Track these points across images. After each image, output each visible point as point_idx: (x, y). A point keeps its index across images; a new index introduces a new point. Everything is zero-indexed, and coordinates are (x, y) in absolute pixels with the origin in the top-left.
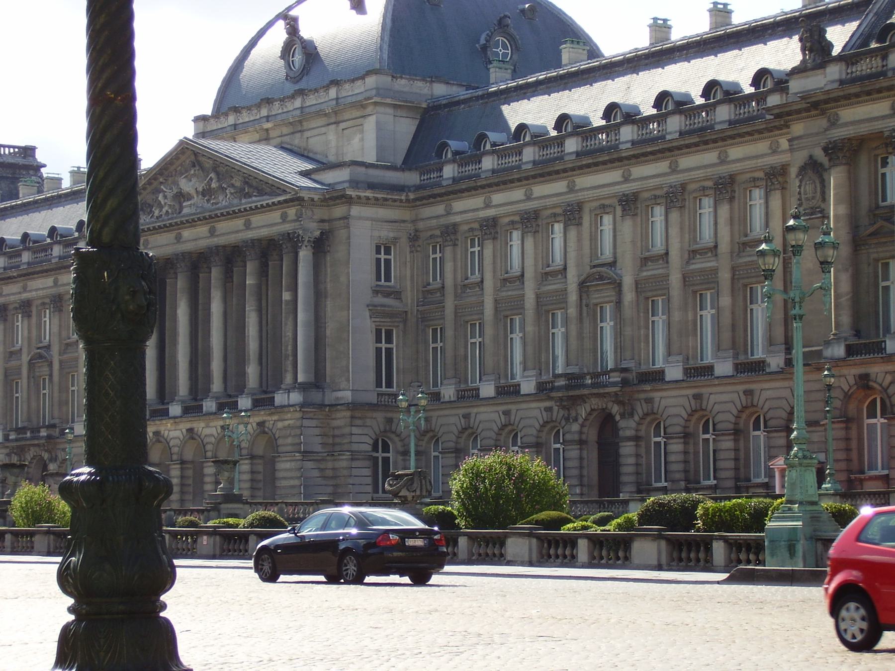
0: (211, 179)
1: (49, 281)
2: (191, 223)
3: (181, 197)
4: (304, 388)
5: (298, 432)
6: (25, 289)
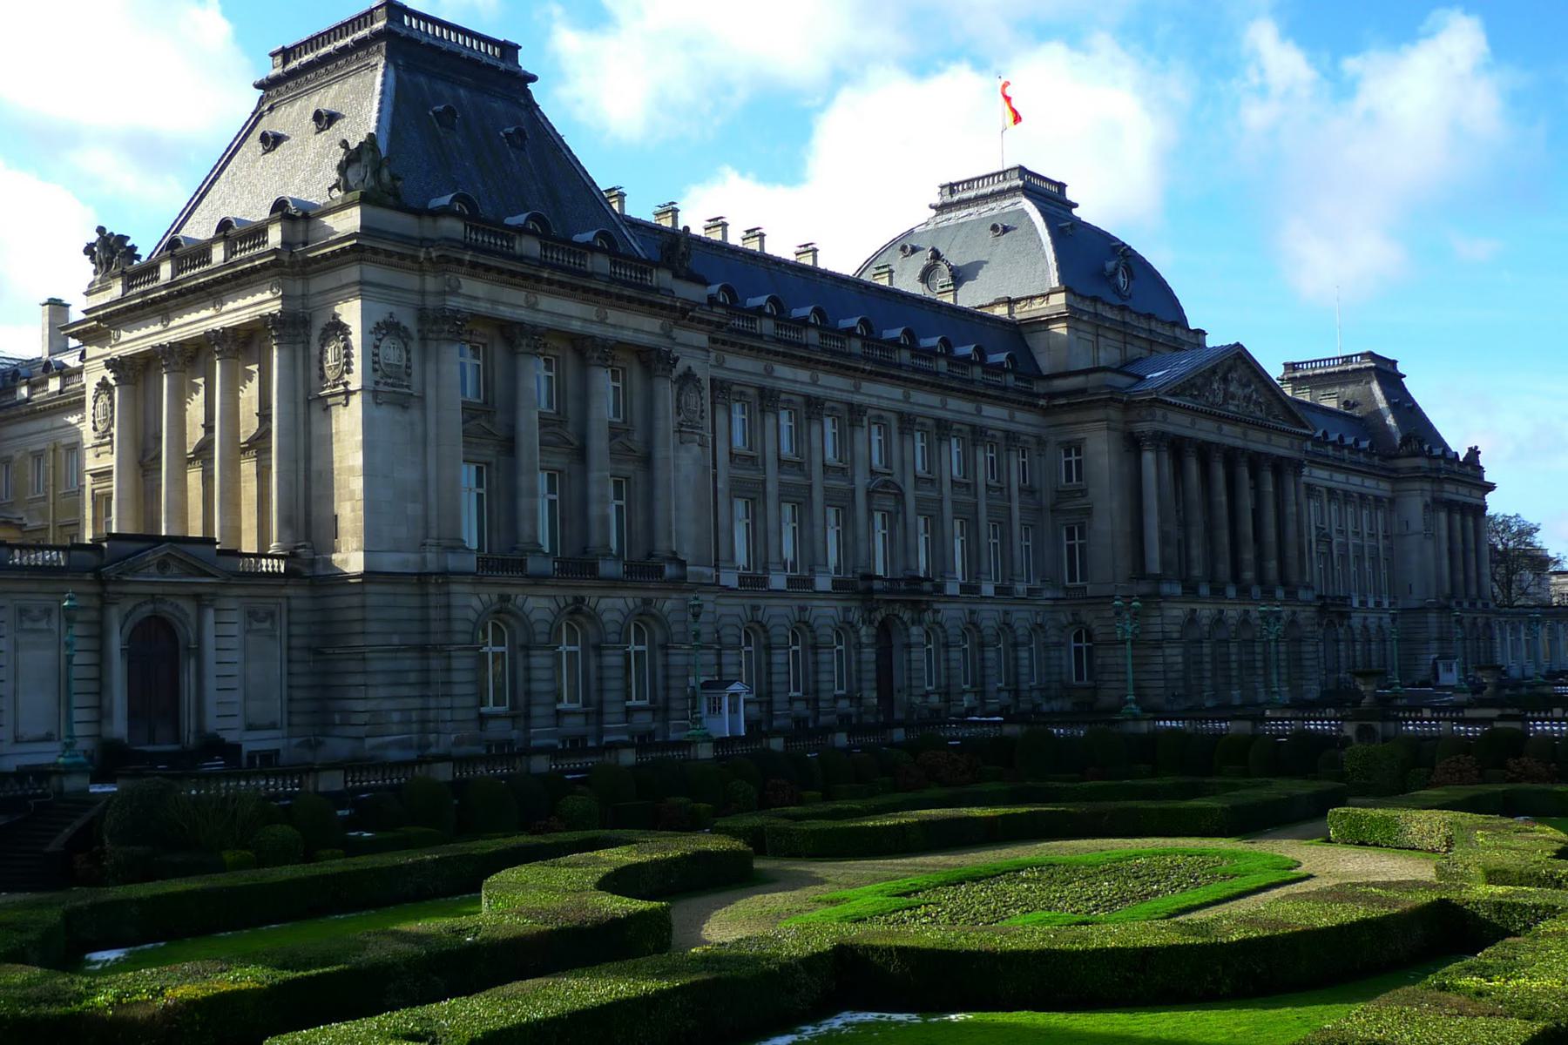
1: (898, 393)
2: (1234, 420)
6: (857, 389)
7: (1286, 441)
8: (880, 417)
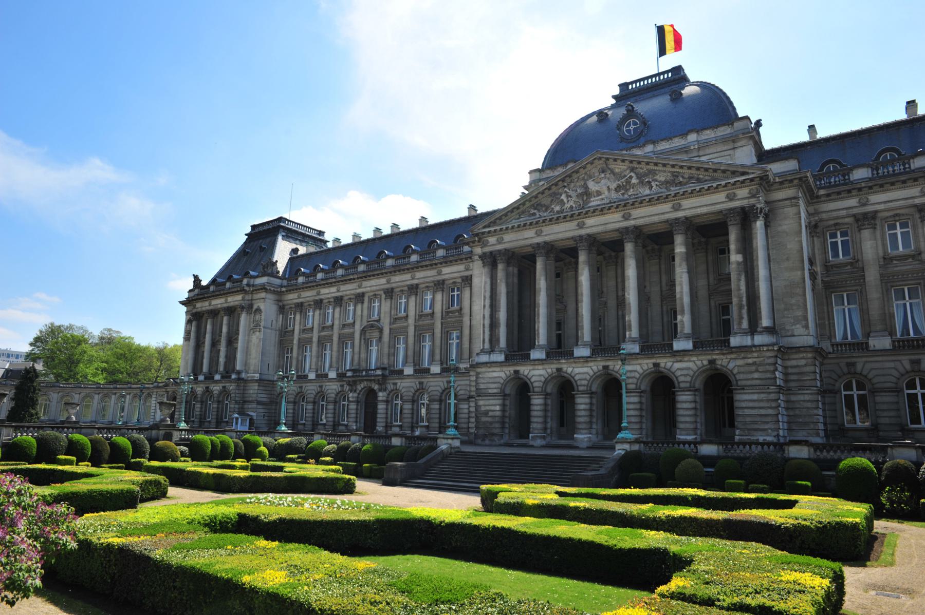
0: (631, 177)
2: (601, 211)
3: (587, 194)
4: (771, 330)
5: (772, 368)
6: (360, 287)
7: (721, 197)
8: (375, 295)
